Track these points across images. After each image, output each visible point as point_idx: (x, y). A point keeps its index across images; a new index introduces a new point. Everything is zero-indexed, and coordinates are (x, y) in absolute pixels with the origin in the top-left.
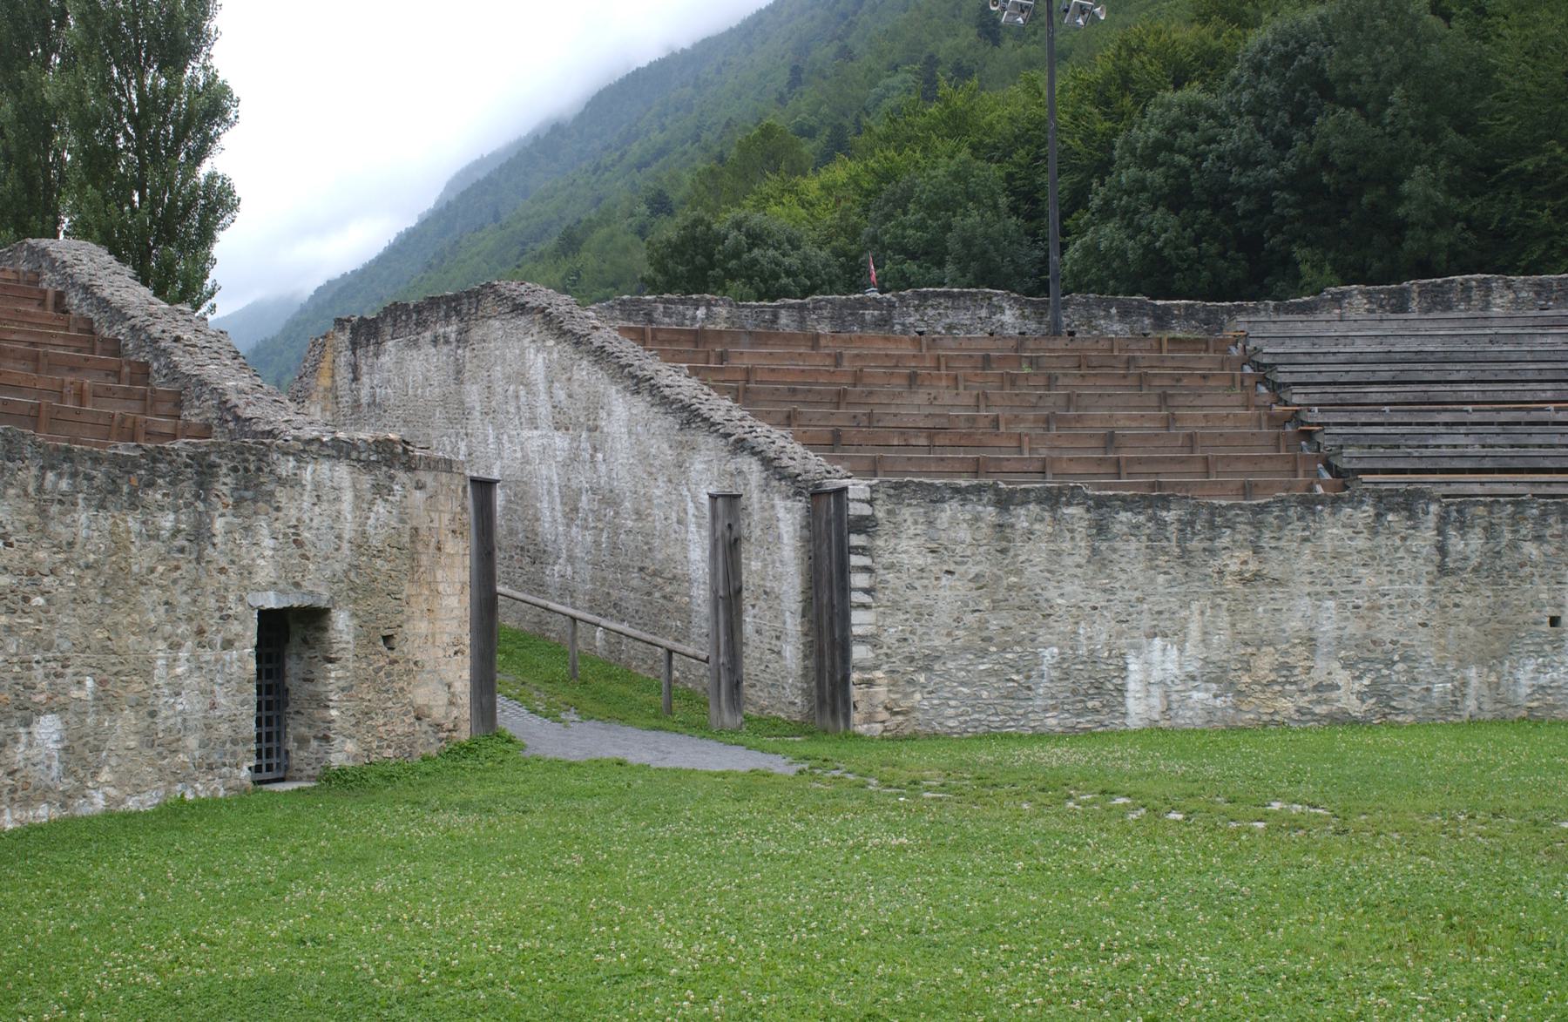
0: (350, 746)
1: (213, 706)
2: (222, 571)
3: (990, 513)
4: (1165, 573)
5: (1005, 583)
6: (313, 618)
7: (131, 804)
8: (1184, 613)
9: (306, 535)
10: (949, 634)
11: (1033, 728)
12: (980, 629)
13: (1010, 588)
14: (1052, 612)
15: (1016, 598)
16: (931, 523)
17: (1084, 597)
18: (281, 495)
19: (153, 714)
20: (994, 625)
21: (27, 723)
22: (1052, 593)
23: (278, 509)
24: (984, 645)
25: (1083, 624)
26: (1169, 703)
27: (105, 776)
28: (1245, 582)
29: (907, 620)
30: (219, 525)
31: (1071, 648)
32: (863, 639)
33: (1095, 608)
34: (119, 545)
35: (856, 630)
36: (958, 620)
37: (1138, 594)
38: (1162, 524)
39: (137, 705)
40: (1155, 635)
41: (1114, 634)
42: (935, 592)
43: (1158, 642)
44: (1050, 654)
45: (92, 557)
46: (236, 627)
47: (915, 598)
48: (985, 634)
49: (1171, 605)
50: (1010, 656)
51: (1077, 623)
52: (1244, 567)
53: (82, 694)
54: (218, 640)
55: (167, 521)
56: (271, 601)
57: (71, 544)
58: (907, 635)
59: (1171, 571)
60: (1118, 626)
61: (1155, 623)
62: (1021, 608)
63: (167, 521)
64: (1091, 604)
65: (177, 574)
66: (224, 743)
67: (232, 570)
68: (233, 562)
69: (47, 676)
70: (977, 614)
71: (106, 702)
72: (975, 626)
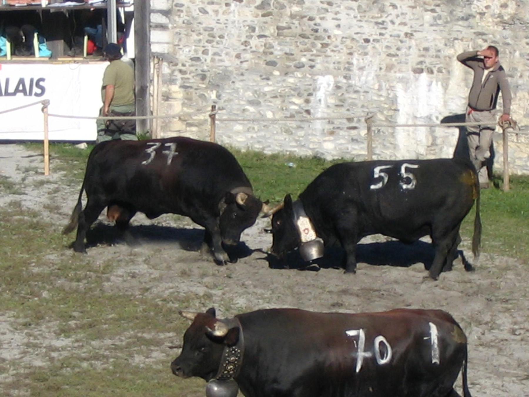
4: (433, 11)
5: (288, 11)
10: (238, 56)
11: (312, 149)
12: (265, 53)
13: (292, 16)
14: (329, 41)
15: (297, 27)
17: (358, 30)
22: (329, 24)
24: (269, 68)
25: (356, 55)
26: (435, 138)
28: (503, 23)
29: (200, 41)
31: (345, 77)
32: (161, 57)
33: (367, 41)
35: (155, 48)
36: (246, 43)
37: (407, 29)
40: (421, 71)
41: (384, 67)
42: (225, 17)
43: (424, 76)
47: (209, 21)
48: (270, 58)
49: (438, 43)
50: (291, 80)
51: (351, 54)
52: (503, 11)
58: (200, 55)
59: (438, 9)
60: (388, 60)
61: (422, 59)
62: (303, 36)
64: (365, 37)
70: (263, 40)
72: (261, 50)
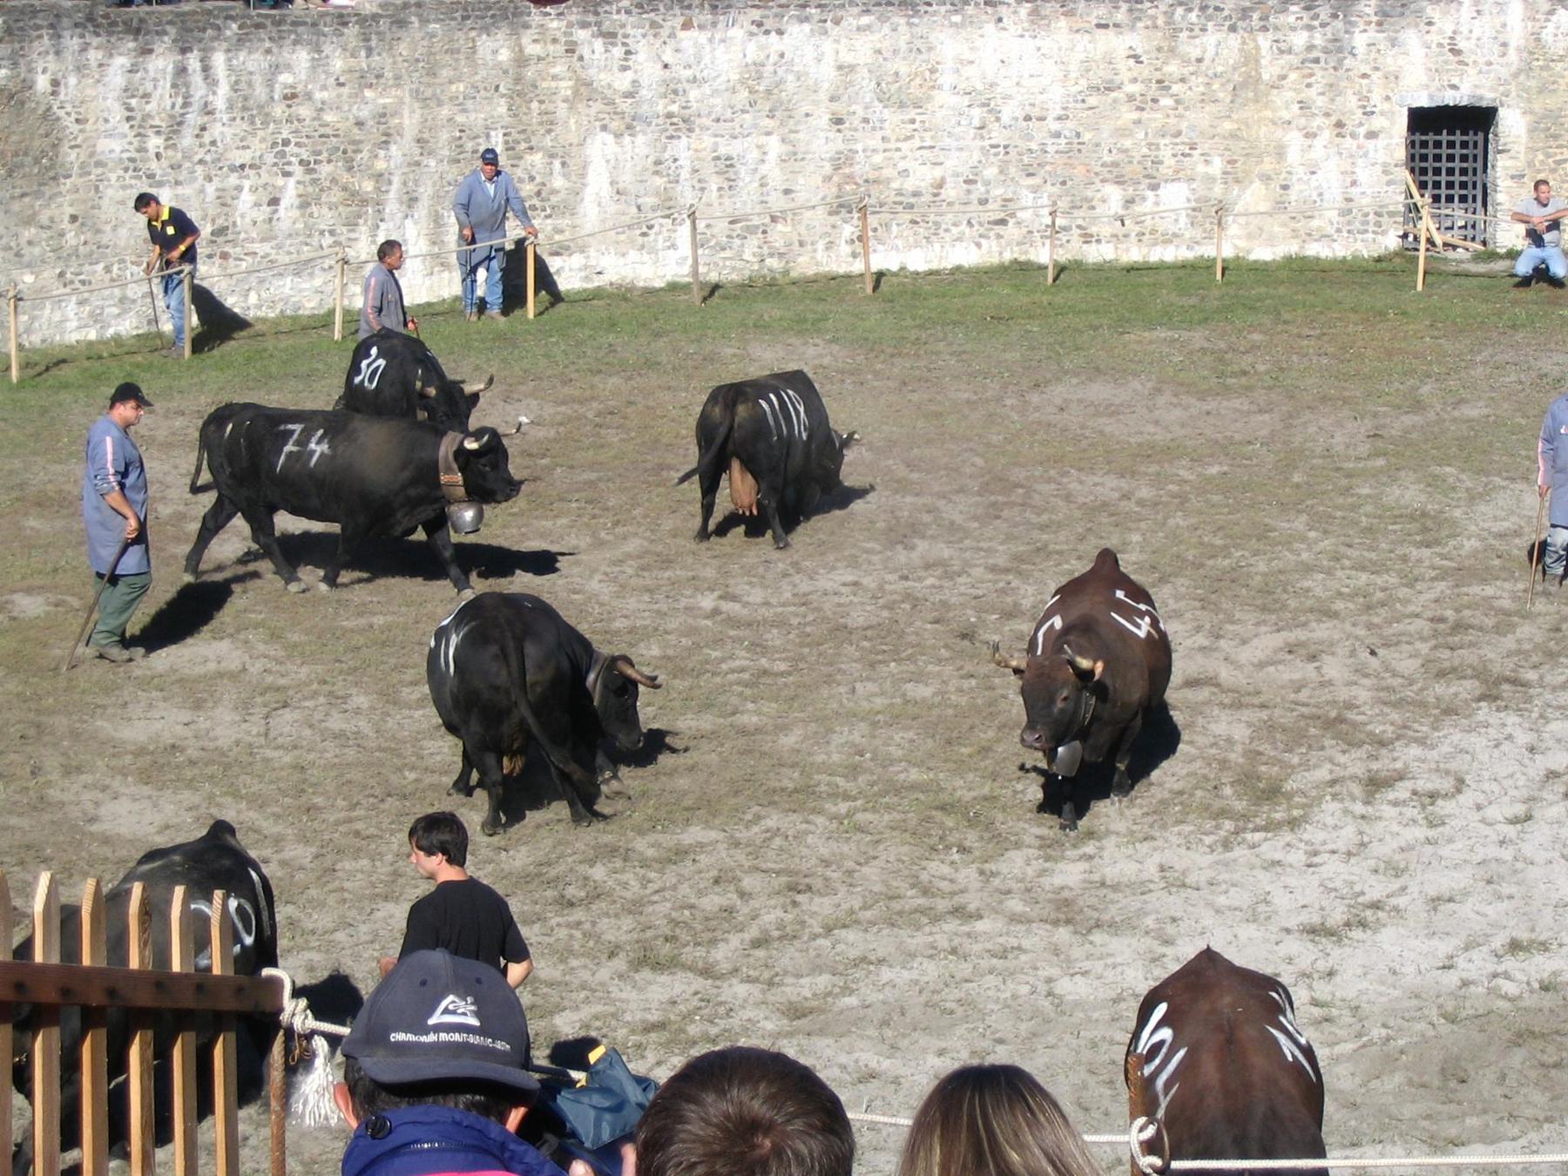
1: (1354, 183)
2: (1365, 76)
9: (1462, 44)
19: (1285, 187)
21: (1154, 188)
23: (1430, 24)
30: (1360, 40)
34: (1251, 59)
39: (1266, 179)
45: (1220, 69)
46: (1377, 123)
54: (1362, 131)
55: (1299, 39)
56: (1424, 102)
57: (1199, 60)
63: (1299, 39)
65: (1312, 80)
66: (1367, 215)
67: (1376, 76)
68: (1377, 69)
69: (1174, 155)
71: (1232, 176)
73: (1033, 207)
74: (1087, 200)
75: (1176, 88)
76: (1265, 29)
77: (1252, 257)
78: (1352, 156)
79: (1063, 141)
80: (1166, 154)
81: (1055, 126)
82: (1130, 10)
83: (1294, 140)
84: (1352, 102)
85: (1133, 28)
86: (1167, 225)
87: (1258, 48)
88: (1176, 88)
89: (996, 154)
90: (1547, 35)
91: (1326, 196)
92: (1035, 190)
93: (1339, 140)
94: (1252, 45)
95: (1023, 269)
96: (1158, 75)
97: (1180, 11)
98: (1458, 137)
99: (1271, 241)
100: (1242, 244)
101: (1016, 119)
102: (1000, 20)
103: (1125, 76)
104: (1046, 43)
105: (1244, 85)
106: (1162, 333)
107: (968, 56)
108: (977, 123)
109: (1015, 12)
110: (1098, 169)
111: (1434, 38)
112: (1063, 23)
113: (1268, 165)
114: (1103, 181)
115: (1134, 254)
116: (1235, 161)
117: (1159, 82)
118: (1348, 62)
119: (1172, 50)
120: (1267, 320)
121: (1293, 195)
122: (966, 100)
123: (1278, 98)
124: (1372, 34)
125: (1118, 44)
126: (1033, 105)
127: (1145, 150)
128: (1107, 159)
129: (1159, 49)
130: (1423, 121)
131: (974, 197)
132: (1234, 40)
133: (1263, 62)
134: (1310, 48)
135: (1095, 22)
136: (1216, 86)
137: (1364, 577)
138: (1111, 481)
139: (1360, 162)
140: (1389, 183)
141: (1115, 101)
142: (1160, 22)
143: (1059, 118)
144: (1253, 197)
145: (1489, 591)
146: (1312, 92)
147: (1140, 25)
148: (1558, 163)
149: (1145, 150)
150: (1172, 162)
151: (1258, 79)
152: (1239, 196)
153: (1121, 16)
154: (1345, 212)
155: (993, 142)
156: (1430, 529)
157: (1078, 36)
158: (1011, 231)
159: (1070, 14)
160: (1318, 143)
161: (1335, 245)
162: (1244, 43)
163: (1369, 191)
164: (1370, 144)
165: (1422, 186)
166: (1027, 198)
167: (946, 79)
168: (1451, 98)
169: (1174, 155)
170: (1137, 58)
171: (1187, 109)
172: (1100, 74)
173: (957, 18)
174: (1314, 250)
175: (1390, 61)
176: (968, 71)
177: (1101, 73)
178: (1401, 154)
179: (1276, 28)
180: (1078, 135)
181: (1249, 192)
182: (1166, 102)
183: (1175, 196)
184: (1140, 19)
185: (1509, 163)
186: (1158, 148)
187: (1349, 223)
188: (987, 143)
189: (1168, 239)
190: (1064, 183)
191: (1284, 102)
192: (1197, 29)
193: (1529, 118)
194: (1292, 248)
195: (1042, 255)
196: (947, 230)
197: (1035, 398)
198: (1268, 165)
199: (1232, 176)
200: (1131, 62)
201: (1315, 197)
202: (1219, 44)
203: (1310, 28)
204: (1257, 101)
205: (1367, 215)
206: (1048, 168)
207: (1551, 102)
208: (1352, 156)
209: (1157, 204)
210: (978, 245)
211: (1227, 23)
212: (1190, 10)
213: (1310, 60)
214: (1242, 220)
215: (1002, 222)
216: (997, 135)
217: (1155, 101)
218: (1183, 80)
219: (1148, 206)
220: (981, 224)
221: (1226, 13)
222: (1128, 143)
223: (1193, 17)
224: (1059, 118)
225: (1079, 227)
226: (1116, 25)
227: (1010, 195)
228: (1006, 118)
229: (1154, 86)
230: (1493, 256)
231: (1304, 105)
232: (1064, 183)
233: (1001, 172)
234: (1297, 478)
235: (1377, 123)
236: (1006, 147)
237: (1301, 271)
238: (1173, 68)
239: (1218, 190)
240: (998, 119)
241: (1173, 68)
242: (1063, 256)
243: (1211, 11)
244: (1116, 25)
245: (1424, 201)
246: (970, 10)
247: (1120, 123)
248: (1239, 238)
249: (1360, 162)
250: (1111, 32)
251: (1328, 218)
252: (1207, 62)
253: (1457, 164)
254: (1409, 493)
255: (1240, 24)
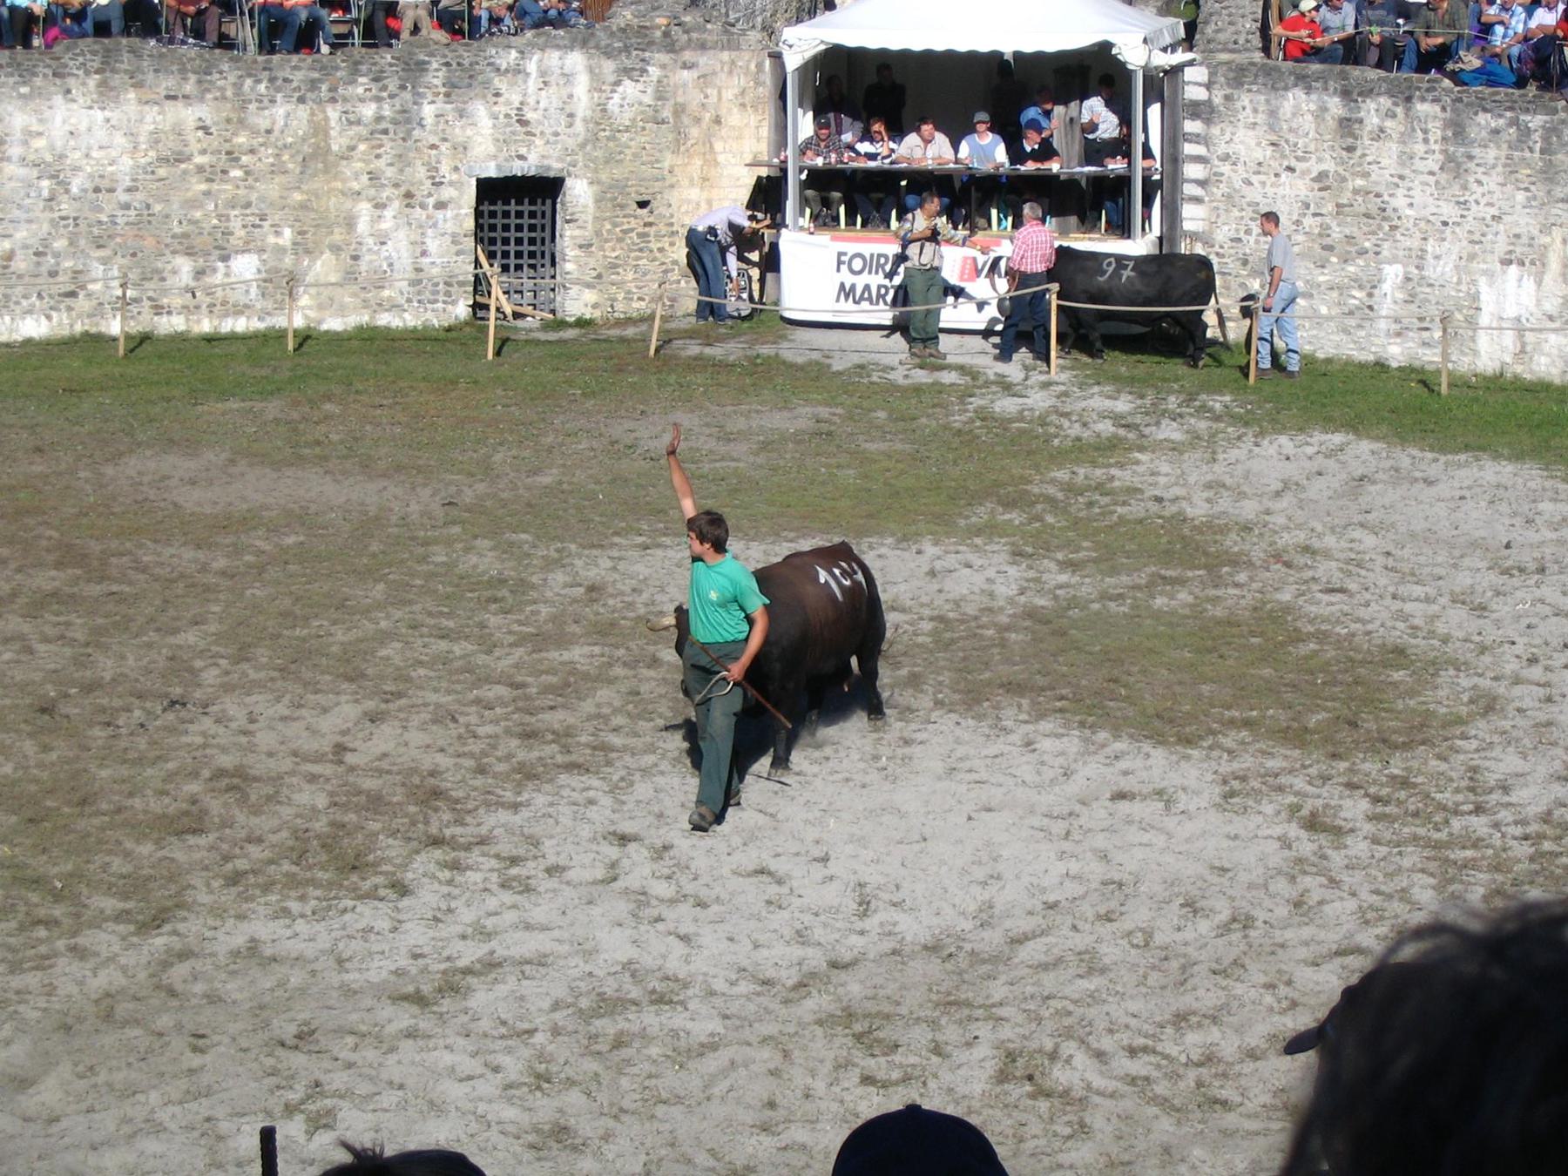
0: (590, 296)
1: (424, 253)
2: (433, 147)
3: (1335, 106)
4: (1527, 190)
6: (546, 189)
7: (334, 324)
8: (1546, 240)
9: (530, 115)
12: (1320, 235)
13: (1356, 192)
15: (1360, 205)
16: (1273, 113)
17: (1435, 210)
18: (499, 83)
19: (355, 258)
20: (1337, 233)
21: (225, 259)
22: (1399, 202)
23: (497, 95)
24: (1325, 253)
25: (1431, 241)
26: (1524, 345)
27: (304, 301)
30: (428, 111)
33: (1445, 224)
34: (320, 130)
36: (1298, 223)
37: (1494, 211)
38: (1526, 132)
39: (336, 249)
40: (1511, 262)
41: (1465, 256)
43: (1513, 268)
44: (1393, 274)
45: (290, 140)
46: (447, 193)
48: (1328, 241)
50: (1351, 269)
53: (280, 241)
54: (431, 201)
55: (368, 111)
56: (492, 172)
57: (269, 132)
58: (1242, 235)
59: (1533, 188)
60: (1470, 248)
62: (1367, 216)
63: (368, 111)
65: (382, 150)
66: (437, 285)
67: (444, 147)
68: (445, 140)
69: (244, 226)
70: (1318, 219)
71: (303, 247)
72: (1316, 231)
73: (103, 278)
74: (157, 271)
75: (245, 159)
76: (333, 100)
77: (324, 327)
78: (421, 227)
79: (133, 213)
80: (236, 225)
81: (124, 197)
82: (199, 82)
83: (364, 209)
84: (421, 172)
85: (202, 99)
86: (237, 296)
87: (327, 119)
88: (245, 159)
89: (65, 227)
90: (613, 105)
91: (396, 267)
92: (105, 261)
93: (408, 210)
94: (321, 116)
95: (95, 342)
96: (227, 146)
97: (249, 82)
98: (526, 208)
99: (342, 311)
100: (312, 314)
101: (85, 191)
102: (68, 91)
103: (194, 147)
104: (114, 115)
105: (314, 156)
106: (234, 404)
107: (36, 128)
108: (45, 193)
109: (84, 84)
110: (169, 240)
111: (501, 109)
112: (132, 95)
113: (338, 236)
114: (174, 252)
115: (206, 326)
116: (305, 233)
117: (228, 153)
118: (417, 133)
119: (241, 122)
120: (338, 390)
121: (363, 266)
122: (35, 173)
123: (347, 170)
124: (440, 105)
125: (189, 115)
126: (102, 177)
127: (215, 221)
128: (178, 230)
129: (228, 121)
130: (490, 190)
131: (44, 269)
132: (303, 112)
133: (333, 133)
134: (379, 119)
135: (164, 93)
136: (286, 157)
137: (443, 645)
138: (189, 553)
139: (430, 232)
140: (458, 253)
141: (185, 172)
142: (229, 93)
143: (129, 190)
144: (323, 267)
145: (566, 656)
146: (381, 163)
147: (209, 96)
148: (625, 232)
149: (215, 221)
150: (242, 233)
151: (329, 149)
152: (309, 267)
153: (189, 87)
154: (415, 283)
155: (63, 213)
156: (493, 591)
157: (147, 108)
158: (82, 303)
159: (138, 85)
160: (389, 213)
161: (406, 315)
162: (313, 114)
163: (438, 261)
164: (440, 214)
165: (491, 256)
166: (98, 270)
167: (15, 151)
168: (518, 169)
169: (244, 226)
170: (205, 129)
171: (256, 180)
172: (169, 145)
173: (24, 90)
174: (385, 319)
175: (458, 132)
176: (40, 143)
177: (171, 145)
178: (470, 224)
179: (345, 100)
180: (148, 207)
181: (319, 263)
182: (236, 173)
183: (245, 266)
184: (208, 90)
185: (577, 232)
186: (228, 220)
187: (419, 293)
188: (57, 215)
189: (239, 310)
190: (134, 255)
191: (354, 173)
192: (266, 100)
193: (595, 187)
194: (365, 319)
195: (114, 327)
196: (17, 303)
197: (109, 471)
198: (338, 236)
199: (303, 247)
200: (200, 133)
201: (385, 267)
202: (288, 115)
203: (378, 99)
204: (326, 171)
205: (437, 285)
206: (118, 240)
207: (617, 172)
208: (421, 227)
209: (227, 275)
210: (49, 318)
211: (297, 95)
212: (259, 81)
213: (378, 131)
214: (313, 291)
215: (73, 294)
216: (66, 207)
217: (224, 172)
218: (252, 151)
219: (218, 278)
220: (50, 296)
221: (295, 84)
222: (198, 214)
223: (262, 88)
224: (129, 190)
225: (150, 299)
226: (185, 97)
227: (81, 267)
228: (75, 190)
229: (224, 157)
230: (561, 324)
231: (373, 176)
232: (134, 255)
233: (71, 244)
234: (375, 547)
235: (447, 193)
236: (75, 219)
237: (370, 339)
238: (241, 139)
239: (288, 261)
240: (67, 191)
241: (241, 139)
242: (135, 328)
243: (279, 82)
244: (185, 97)
245: (491, 270)
246: (38, 81)
247: (190, 194)
248: (310, 308)
249: (430, 232)
250: (180, 104)
251: (396, 290)
252: (276, 133)
253: (525, 234)
254: (484, 560)
255: (309, 95)
